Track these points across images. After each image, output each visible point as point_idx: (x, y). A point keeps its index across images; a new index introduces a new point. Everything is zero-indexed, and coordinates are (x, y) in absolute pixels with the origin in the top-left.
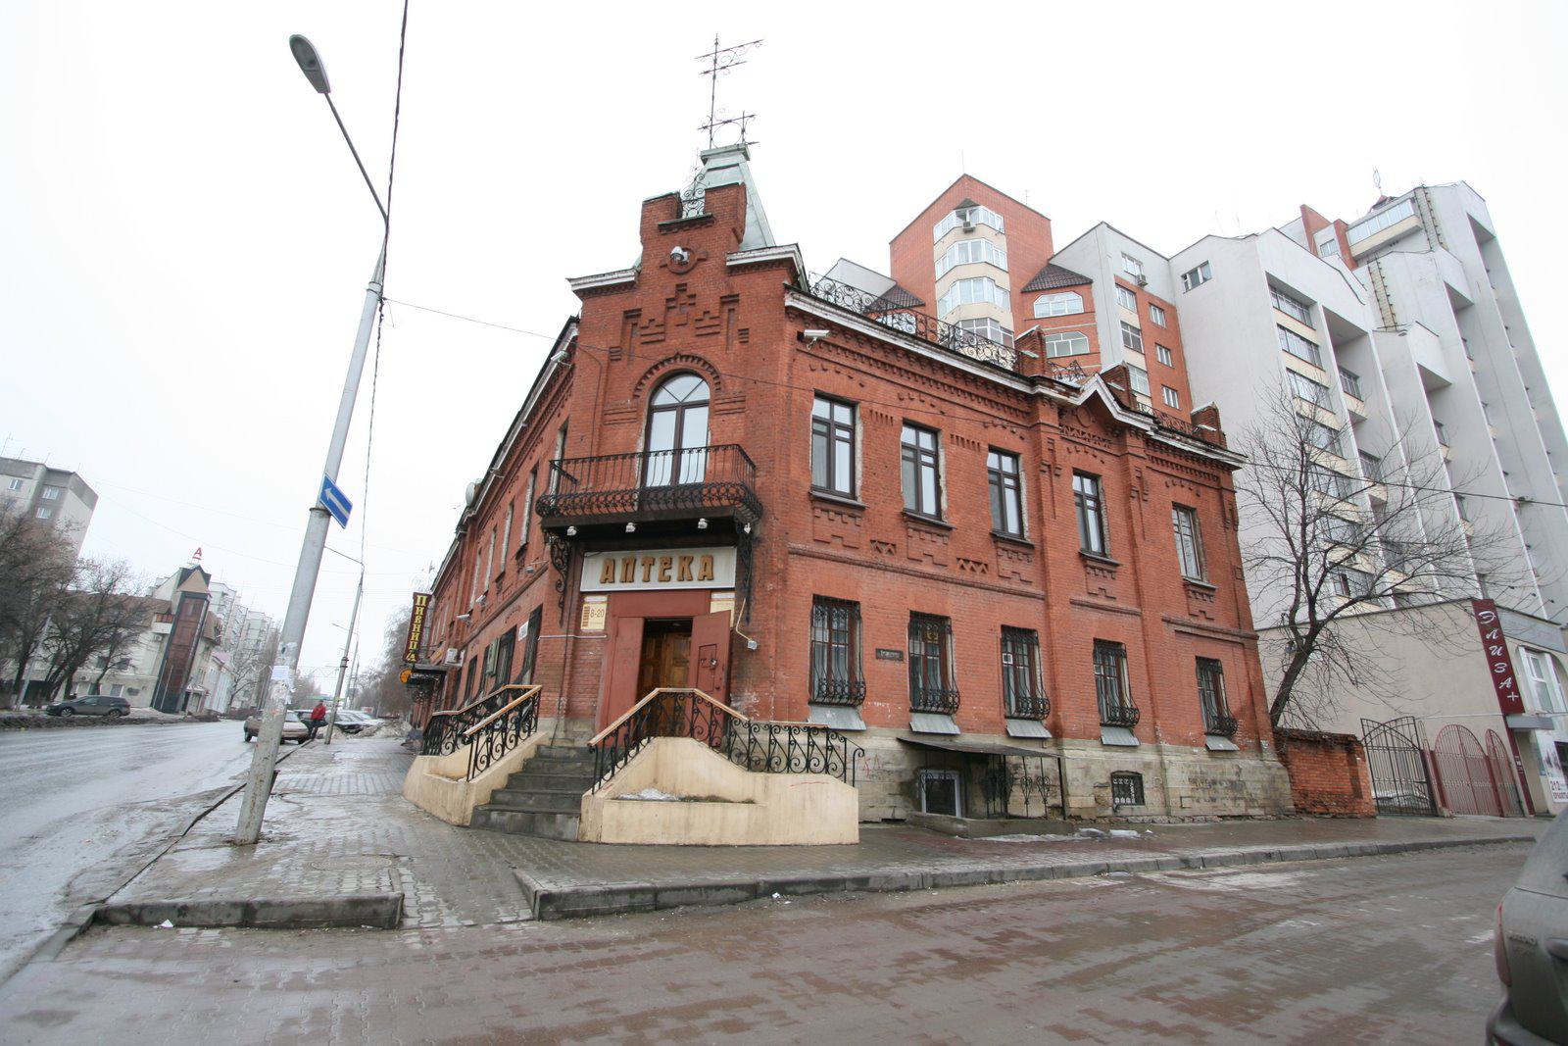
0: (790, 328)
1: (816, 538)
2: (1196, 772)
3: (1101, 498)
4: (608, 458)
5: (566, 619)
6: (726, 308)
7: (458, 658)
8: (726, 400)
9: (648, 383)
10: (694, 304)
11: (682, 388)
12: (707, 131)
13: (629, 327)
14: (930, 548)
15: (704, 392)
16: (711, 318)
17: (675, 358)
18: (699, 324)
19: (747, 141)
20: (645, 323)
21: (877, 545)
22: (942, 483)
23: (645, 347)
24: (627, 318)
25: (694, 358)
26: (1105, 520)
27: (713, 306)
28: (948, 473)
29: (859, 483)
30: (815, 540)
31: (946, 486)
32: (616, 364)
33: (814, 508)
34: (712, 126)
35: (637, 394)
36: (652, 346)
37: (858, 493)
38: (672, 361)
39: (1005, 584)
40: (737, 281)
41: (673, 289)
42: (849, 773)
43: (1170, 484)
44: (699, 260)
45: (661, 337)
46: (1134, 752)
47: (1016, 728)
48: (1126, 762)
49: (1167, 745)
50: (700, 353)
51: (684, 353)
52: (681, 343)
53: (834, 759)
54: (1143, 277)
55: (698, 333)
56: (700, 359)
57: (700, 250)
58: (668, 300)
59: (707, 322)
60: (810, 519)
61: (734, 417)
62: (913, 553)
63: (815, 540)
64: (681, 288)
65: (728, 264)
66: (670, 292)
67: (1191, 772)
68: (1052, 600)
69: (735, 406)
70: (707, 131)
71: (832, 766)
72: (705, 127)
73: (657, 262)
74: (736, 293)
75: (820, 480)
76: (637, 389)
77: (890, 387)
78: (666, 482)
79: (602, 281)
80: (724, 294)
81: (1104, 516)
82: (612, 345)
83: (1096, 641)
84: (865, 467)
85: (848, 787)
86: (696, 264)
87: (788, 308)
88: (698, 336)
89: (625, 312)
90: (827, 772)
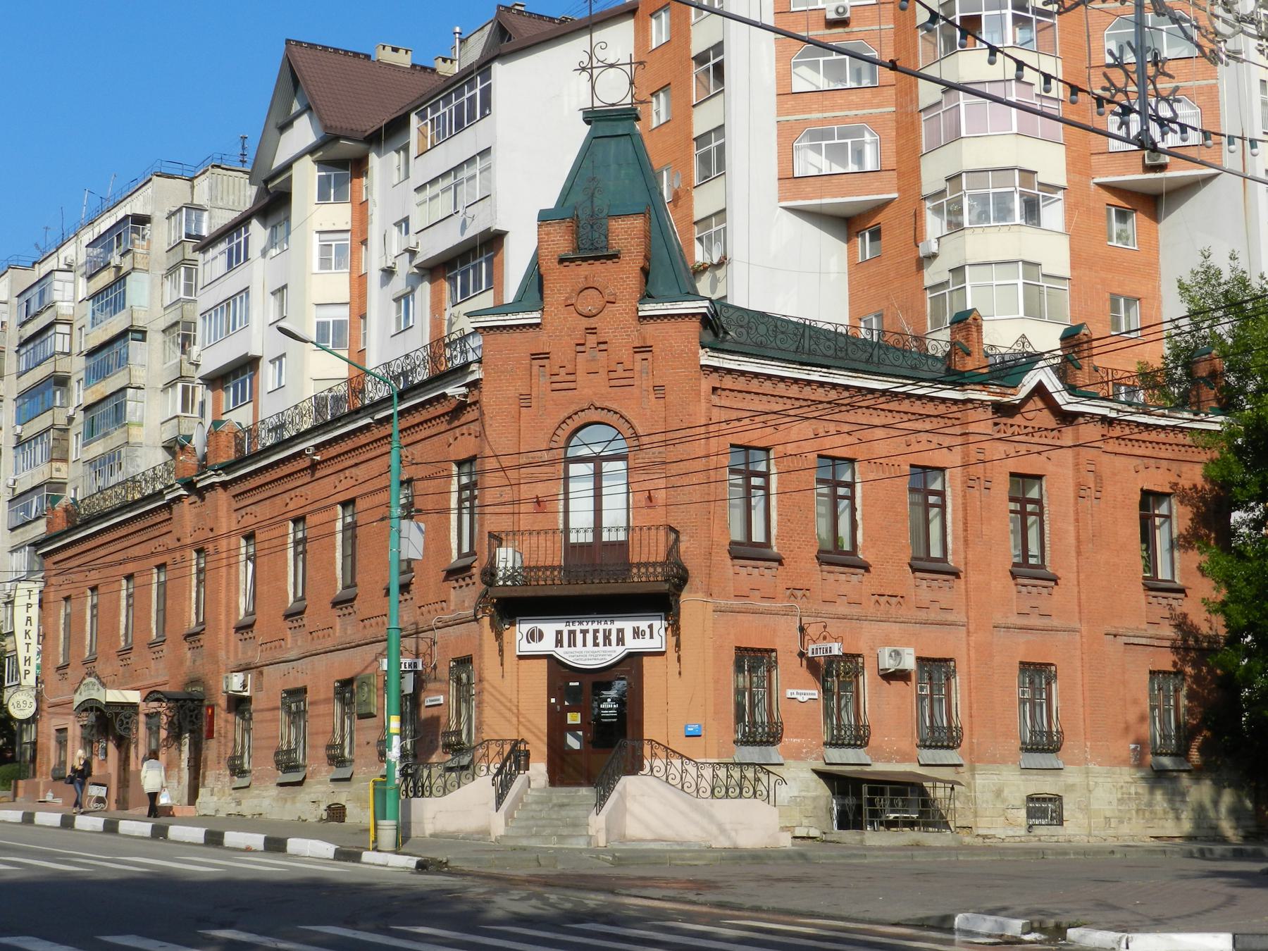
0: (706, 384)
2: (1130, 794)
3: (1045, 501)
7: (244, 686)
12: (585, 75)
18: (613, 375)
21: (793, 591)
26: (1047, 528)
27: (625, 354)
28: (864, 505)
29: (774, 531)
31: (862, 519)
34: (592, 68)
37: (773, 542)
39: (923, 615)
40: (650, 328)
41: (583, 332)
42: (772, 798)
43: (1141, 468)
45: (572, 385)
46: (1058, 775)
47: (928, 755)
48: (1045, 785)
49: (1097, 767)
50: (614, 406)
51: (598, 405)
53: (760, 787)
55: (613, 383)
56: (616, 413)
59: (620, 373)
62: (828, 597)
65: (641, 314)
66: (578, 335)
67: (1123, 794)
68: (972, 628)
70: (585, 75)
71: (759, 793)
72: (583, 69)
75: (737, 534)
78: (589, 538)
81: (1046, 522)
82: (523, 393)
83: (1021, 663)
84: (779, 515)
85: (770, 808)
87: (702, 366)
90: (755, 797)
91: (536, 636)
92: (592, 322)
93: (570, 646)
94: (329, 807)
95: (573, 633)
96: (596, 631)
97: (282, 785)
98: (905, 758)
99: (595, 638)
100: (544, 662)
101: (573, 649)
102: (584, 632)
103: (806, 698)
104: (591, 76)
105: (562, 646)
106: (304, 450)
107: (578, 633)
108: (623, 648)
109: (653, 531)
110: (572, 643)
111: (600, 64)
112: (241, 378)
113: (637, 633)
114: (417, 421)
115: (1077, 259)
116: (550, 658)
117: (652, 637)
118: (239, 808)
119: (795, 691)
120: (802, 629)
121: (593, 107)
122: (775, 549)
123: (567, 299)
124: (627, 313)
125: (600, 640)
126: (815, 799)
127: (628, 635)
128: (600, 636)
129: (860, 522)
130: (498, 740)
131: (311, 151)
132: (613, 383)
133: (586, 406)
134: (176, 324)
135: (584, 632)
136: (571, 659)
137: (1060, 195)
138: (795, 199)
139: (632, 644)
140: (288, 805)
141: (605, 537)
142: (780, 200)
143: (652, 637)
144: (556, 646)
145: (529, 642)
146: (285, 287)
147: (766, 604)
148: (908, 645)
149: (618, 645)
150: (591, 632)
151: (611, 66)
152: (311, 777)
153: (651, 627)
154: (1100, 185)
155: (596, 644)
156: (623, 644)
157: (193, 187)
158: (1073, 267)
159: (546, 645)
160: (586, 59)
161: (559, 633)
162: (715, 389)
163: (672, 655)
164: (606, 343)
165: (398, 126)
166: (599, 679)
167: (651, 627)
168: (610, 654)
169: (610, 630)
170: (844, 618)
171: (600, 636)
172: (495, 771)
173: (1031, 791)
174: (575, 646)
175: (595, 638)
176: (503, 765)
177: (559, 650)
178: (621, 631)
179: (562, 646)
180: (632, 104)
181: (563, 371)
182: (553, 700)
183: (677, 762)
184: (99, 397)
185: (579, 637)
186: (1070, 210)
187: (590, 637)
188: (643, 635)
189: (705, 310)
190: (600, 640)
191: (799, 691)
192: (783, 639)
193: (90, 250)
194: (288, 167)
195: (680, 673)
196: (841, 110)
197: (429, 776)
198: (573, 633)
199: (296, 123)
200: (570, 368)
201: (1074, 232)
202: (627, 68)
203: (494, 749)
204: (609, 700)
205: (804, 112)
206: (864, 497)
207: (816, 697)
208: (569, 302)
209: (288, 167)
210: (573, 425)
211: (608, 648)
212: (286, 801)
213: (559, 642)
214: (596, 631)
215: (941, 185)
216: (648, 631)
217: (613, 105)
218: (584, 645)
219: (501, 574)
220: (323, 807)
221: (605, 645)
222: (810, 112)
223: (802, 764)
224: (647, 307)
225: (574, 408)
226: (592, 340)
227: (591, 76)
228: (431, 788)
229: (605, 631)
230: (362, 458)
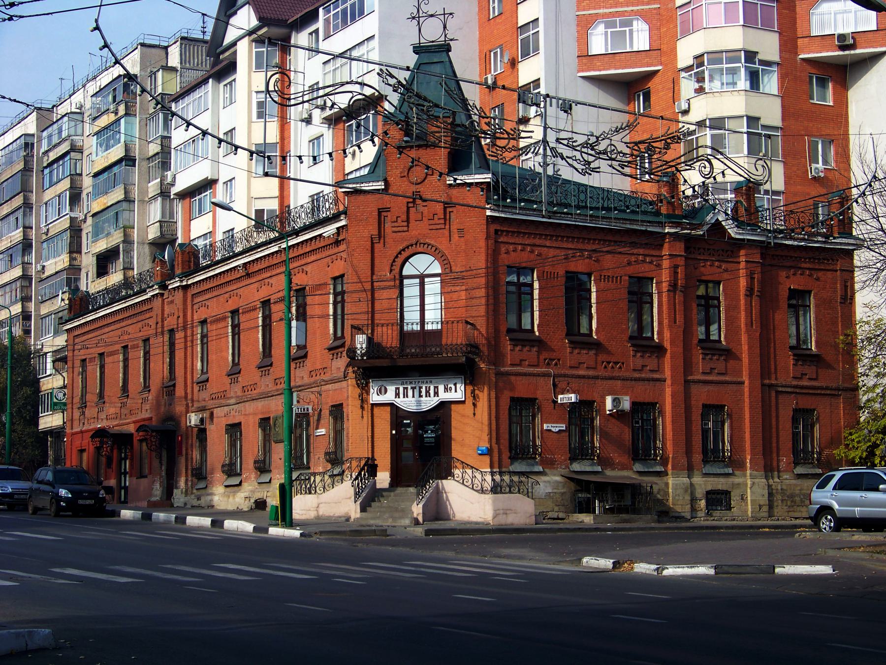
5: (365, 416)
11: (421, 263)
12: (415, 22)
15: (437, 268)
17: (416, 244)
19: (449, 36)
29: (536, 322)
34: (419, 17)
40: (455, 192)
42: (530, 494)
45: (406, 229)
48: (720, 484)
52: (419, 234)
55: (431, 227)
70: (415, 22)
72: (414, 18)
83: (703, 405)
87: (488, 216)
93: (404, 397)
94: (256, 501)
97: (226, 486)
98: (624, 467)
100: (388, 409)
101: (406, 399)
103: (557, 429)
104: (419, 22)
105: (399, 397)
106: (237, 266)
108: (438, 398)
109: (455, 324)
110: (406, 395)
111: (424, 15)
112: (203, 195)
113: (446, 389)
114: (308, 250)
115: (786, 114)
116: (392, 405)
117: (456, 391)
118: (199, 502)
120: (555, 385)
121: (420, 43)
122: (537, 334)
123: (401, 173)
125: (423, 393)
126: (563, 494)
127: (441, 388)
128: (423, 390)
131: (250, 33)
132: (431, 227)
133: (414, 242)
134: (157, 154)
135: (413, 388)
137: (775, 68)
138: (589, 70)
139: (444, 396)
140: (231, 499)
141: (429, 327)
142: (579, 71)
143: (456, 391)
146: (234, 129)
147: (531, 370)
148: (626, 394)
150: (418, 388)
151: (432, 16)
152: (245, 482)
154: (803, 59)
156: (438, 396)
157: (167, 54)
158: (783, 119)
159: (389, 396)
160: (415, 11)
162: (496, 231)
163: (469, 402)
165: (312, 16)
166: (423, 419)
168: (429, 403)
170: (584, 377)
171: (423, 390)
172: (354, 477)
173: (709, 488)
175: (420, 392)
176: (360, 474)
177: (397, 400)
180: (445, 41)
182: (394, 432)
183: (469, 471)
184: (102, 207)
185: (410, 392)
186: (782, 79)
188: (451, 390)
189: (488, 180)
190: (423, 393)
192: (541, 390)
193: (94, 99)
194: (234, 44)
195: (474, 414)
196: (622, 7)
197: (314, 481)
199: (238, 12)
201: (786, 95)
202: (442, 17)
203: (355, 464)
205: (595, 9)
207: (564, 428)
208: (403, 175)
209: (234, 44)
210: (405, 255)
211: (428, 398)
212: (229, 497)
213: (397, 395)
214: (420, 388)
215: (690, 62)
216: (453, 387)
217: (433, 42)
219: (359, 352)
220: (252, 501)
221: (426, 396)
222: (600, 8)
223: (555, 471)
227: (419, 22)
228: (315, 488)
229: (426, 387)
230: (274, 273)
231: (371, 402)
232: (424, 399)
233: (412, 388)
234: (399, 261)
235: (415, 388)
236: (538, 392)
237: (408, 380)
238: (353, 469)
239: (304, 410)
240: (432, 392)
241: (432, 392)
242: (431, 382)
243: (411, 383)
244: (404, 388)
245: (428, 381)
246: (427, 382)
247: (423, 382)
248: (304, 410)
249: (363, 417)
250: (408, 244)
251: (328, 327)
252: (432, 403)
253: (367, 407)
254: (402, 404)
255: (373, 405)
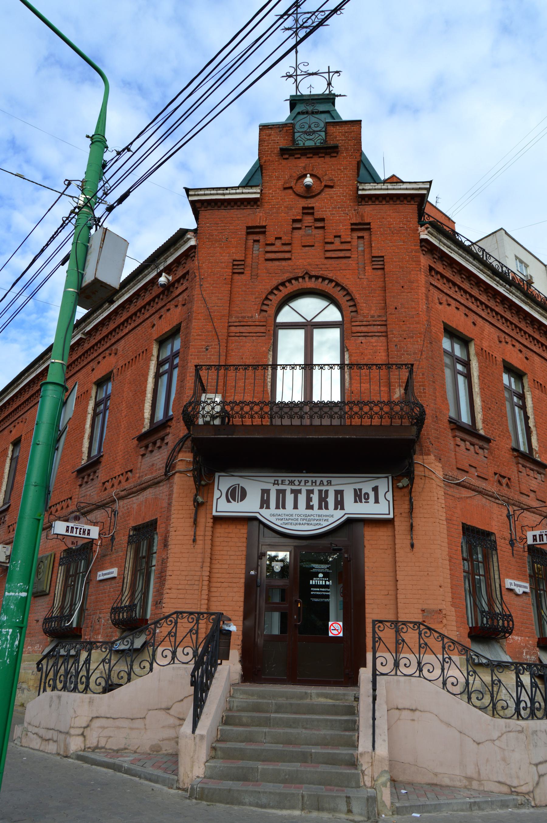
0: (425, 261)
1: (460, 467)
4: (236, 367)
6: (356, 234)
8: (365, 323)
9: (275, 299)
10: (323, 228)
12: (292, 80)
13: (250, 242)
14: (534, 484)
16: (342, 243)
17: (303, 278)
18: (329, 247)
20: (271, 240)
22: (531, 424)
23: (269, 264)
24: (248, 233)
25: (324, 279)
27: (344, 230)
28: (535, 414)
29: (479, 417)
30: (458, 469)
31: (535, 426)
32: (236, 276)
33: (454, 437)
34: (297, 75)
35: (265, 307)
36: (277, 263)
38: (300, 280)
44: (326, 186)
45: (287, 255)
50: (330, 275)
51: (313, 273)
54: (531, 277)
55: (329, 254)
56: (331, 281)
57: (326, 178)
58: (294, 221)
59: (337, 244)
60: (452, 446)
61: (374, 340)
63: (458, 469)
64: (308, 211)
65: (360, 192)
66: (296, 213)
69: (375, 329)
72: (290, 76)
73: (281, 183)
74: (367, 221)
76: (263, 304)
77: (493, 330)
79: (224, 194)
80: (354, 221)
82: (237, 259)
84: (483, 401)
86: (322, 191)
88: (326, 258)
89: (248, 228)
91: (238, 494)
92: (310, 203)
93: (277, 507)
95: (281, 493)
96: (309, 492)
99: (309, 499)
101: (281, 511)
102: (296, 493)
105: (268, 507)
107: (288, 493)
108: (343, 512)
110: (281, 504)
111: (303, 73)
113: (359, 496)
117: (377, 501)
119: (513, 581)
124: (345, 196)
129: (533, 429)
130: (191, 613)
132: (329, 254)
135: (296, 493)
136: (279, 523)
143: (377, 501)
144: (262, 507)
145: (228, 501)
149: (336, 508)
150: (304, 493)
153: (375, 489)
155: (309, 507)
156: (342, 508)
161: (265, 492)
164: (323, 220)
167: (375, 489)
169: (327, 492)
174: (284, 507)
175: (309, 499)
177: (264, 512)
178: (339, 493)
179: (268, 507)
181: (278, 243)
185: (290, 499)
187: (302, 499)
191: (517, 582)
195: (412, 546)
197: (88, 661)
198: (281, 493)
200: (286, 239)
202: (326, 75)
203: (184, 626)
204: (321, 575)
206: (535, 408)
207: (528, 590)
211: (324, 512)
213: (265, 503)
214: (309, 492)
218: (296, 507)
221: (320, 508)
224: (367, 186)
225: (285, 277)
226: (308, 220)
227: (296, 80)
228: (88, 678)
229: (320, 492)
231: (214, 513)
232: (316, 511)
233: (293, 491)
234: (275, 299)
235: (300, 491)
236: (494, 523)
237: (287, 477)
238: (179, 640)
239: (84, 532)
240: (331, 500)
241: (331, 500)
242: (329, 483)
243: (292, 483)
244: (279, 492)
245: (325, 481)
246: (322, 483)
247: (314, 483)
248: (84, 532)
249: (194, 541)
250: (292, 276)
251: (141, 410)
252: (331, 520)
253: (205, 522)
254: (273, 519)
255: (218, 520)
